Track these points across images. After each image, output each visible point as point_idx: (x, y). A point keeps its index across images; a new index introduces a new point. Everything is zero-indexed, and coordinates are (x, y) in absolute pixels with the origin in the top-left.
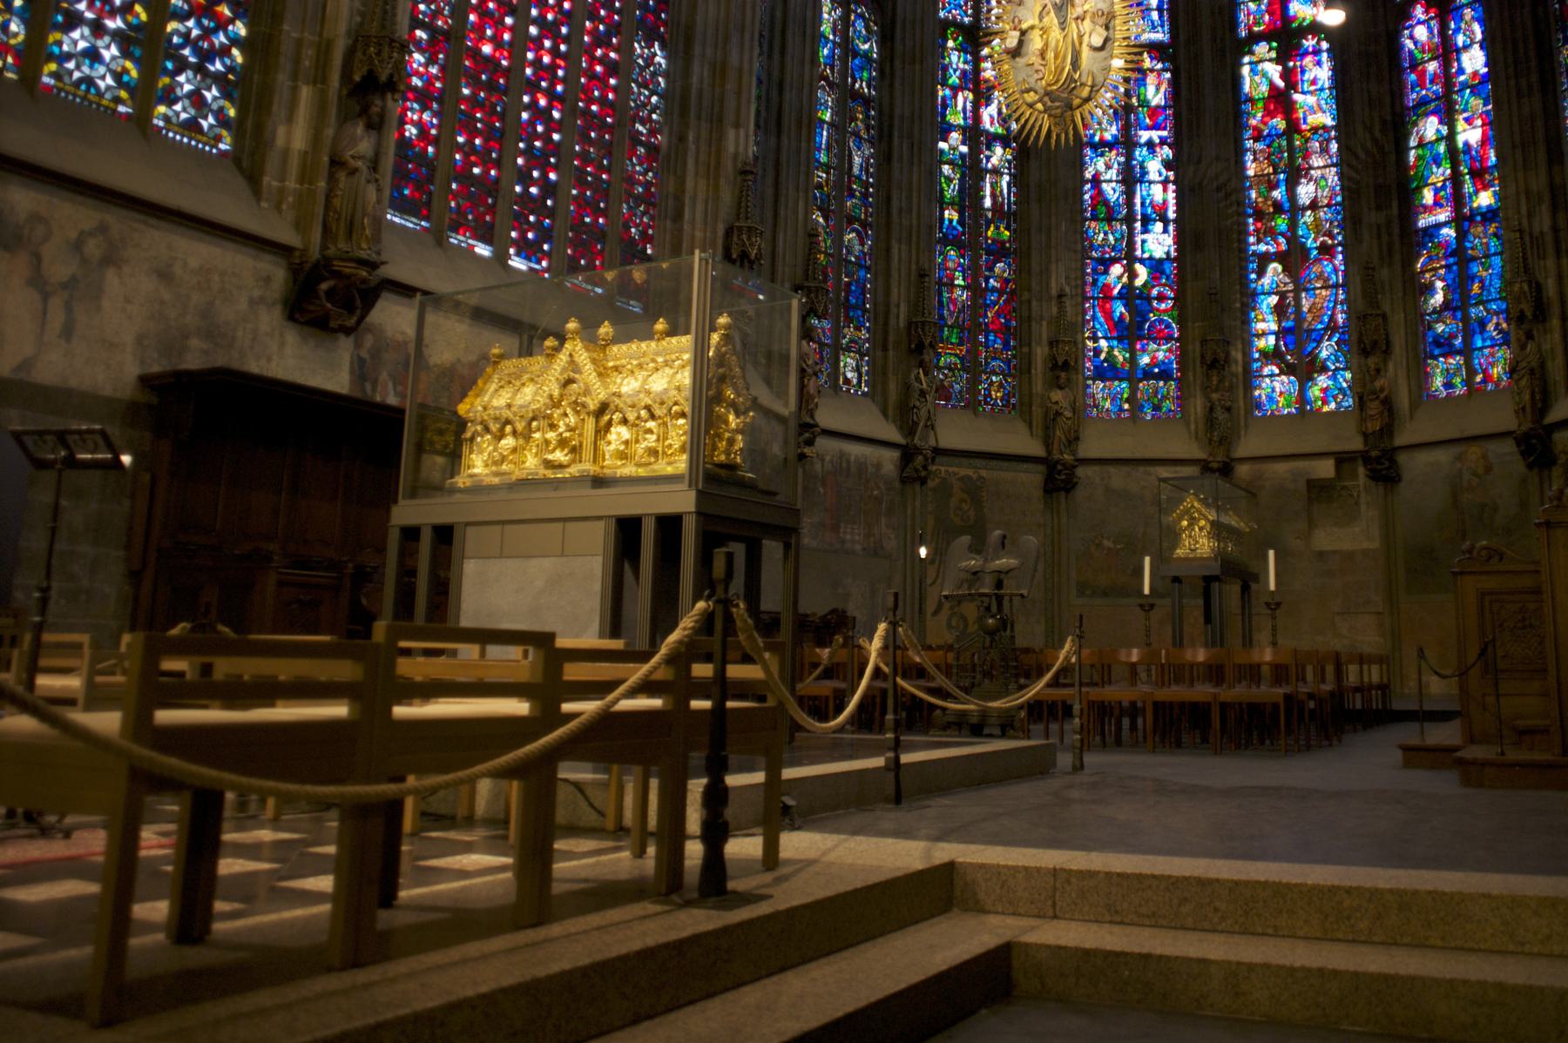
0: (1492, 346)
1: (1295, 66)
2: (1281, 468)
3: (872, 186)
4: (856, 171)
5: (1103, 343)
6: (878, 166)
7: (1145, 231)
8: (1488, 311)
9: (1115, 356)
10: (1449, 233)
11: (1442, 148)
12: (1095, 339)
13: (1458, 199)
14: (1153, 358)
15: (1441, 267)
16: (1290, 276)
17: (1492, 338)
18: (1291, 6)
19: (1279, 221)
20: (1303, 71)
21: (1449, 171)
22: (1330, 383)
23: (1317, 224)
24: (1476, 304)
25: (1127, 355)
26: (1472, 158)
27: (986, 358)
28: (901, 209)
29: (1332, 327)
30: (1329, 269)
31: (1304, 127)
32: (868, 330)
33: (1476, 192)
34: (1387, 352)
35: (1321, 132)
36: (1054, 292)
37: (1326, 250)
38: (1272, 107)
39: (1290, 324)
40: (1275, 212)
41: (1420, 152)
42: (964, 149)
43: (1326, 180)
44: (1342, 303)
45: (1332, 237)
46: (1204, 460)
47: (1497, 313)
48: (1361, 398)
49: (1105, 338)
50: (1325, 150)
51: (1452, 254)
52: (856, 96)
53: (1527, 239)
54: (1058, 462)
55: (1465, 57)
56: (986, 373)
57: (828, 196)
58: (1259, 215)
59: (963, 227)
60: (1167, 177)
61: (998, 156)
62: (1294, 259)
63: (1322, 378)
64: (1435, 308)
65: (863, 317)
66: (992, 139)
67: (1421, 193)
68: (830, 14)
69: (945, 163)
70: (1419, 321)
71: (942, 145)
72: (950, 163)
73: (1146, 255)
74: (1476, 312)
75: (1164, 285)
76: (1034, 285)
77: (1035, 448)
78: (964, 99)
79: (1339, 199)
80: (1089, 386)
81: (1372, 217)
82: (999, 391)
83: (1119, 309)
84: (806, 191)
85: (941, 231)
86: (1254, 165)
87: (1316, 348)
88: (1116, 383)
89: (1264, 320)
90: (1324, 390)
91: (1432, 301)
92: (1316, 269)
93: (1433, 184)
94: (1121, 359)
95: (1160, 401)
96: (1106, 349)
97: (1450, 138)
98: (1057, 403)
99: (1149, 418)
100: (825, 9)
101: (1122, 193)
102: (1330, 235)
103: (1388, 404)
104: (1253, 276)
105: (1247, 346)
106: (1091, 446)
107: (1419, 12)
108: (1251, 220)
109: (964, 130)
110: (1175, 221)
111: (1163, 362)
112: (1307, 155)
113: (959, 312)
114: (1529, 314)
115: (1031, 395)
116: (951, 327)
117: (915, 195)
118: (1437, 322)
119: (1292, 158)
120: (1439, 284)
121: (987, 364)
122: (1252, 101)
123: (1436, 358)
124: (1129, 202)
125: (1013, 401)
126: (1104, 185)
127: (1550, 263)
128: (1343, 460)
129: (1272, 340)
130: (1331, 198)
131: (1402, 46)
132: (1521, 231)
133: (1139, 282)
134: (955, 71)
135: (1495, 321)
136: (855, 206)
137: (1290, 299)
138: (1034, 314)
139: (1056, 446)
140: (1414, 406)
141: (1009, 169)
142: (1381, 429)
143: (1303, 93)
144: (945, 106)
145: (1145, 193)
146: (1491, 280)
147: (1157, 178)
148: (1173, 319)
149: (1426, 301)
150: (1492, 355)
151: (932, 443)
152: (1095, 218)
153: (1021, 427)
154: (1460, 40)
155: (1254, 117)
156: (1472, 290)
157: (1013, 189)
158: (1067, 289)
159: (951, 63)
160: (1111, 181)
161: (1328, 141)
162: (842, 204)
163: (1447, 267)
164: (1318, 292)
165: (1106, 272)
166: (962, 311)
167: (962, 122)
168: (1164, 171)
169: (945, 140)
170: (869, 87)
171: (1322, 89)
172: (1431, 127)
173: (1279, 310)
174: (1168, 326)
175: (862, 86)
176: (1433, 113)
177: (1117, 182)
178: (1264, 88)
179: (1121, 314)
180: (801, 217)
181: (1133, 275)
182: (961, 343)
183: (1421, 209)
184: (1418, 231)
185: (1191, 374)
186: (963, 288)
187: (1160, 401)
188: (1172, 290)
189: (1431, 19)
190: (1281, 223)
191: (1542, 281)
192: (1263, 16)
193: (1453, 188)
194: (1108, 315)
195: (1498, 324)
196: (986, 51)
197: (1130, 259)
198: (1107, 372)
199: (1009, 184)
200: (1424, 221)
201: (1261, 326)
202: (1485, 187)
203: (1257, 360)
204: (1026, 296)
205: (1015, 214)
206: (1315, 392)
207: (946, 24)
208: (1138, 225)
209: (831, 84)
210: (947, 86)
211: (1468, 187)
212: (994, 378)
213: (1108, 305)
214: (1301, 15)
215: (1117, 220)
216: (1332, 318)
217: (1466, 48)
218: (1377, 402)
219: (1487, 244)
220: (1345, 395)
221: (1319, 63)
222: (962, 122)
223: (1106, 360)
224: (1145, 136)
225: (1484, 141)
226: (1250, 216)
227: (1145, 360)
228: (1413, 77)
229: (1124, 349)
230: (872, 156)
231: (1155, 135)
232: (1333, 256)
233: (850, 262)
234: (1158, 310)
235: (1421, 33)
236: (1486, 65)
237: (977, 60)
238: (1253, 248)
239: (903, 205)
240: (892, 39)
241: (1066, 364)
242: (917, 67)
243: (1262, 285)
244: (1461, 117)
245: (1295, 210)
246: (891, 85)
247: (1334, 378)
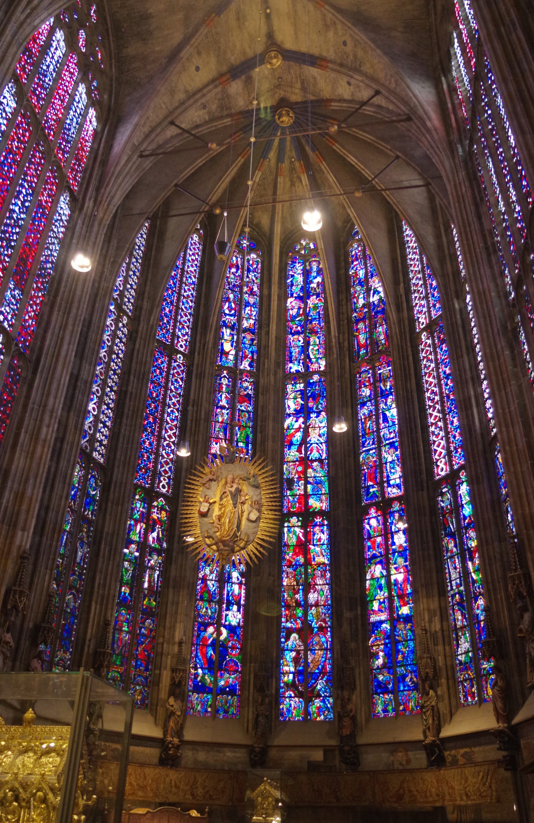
0: (408, 690)
1: (310, 531)
2: (294, 754)
3: (85, 569)
4: (78, 560)
5: (200, 671)
6: (91, 558)
7: (228, 609)
8: (406, 670)
9: (206, 679)
10: (386, 626)
11: (383, 581)
12: (196, 668)
13: (391, 609)
14: (227, 682)
15: (382, 644)
16: (303, 642)
17: (409, 686)
18: (310, 501)
19: (298, 611)
20: (314, 535)
21: (386, 594)
22: (321, 704)
23: (318, 615)
24: (400, 666)
25: (212, 679)
26: (398, 588)
27: (134, 675)
28: (99, 584)
29: (322, 672)
30: (323, 639)
31: (313, 563)
32: (71, 653)
33: (401, 606)
34: (354, 689)
35: (321, 566)
36: (177, 640)
37: (321, 628)
38: (297, 551)
39: (301, 668)
40: (296, 606)
41: (372, 582)
42: (137, 554)
43: (323, 592)
44: (329, 660)
45: (326, 623)
46: (252, 746)
47: (411, 672)
48: (339, 715)
49: (202, 668)
50: (323, 576)
51: (388, 637)
52: (85, 519)
53: (428, 634)
54: (170, 742)
55: (396, 537)
56: (133, 684)
57: (62, 572)
58: (288, 607)
59: (131, 598)
60: (241, 581)
61: (154, 560)
63: (317, 701)
64: (378, 666)
65: (69, 644)
66: (153, 550)
67: (372, 603)
68: (78, 473)
69: (126, 561)
71: (126, 551)
72: (129, 561)
73: (227, 623)
74: (401, 670)
75: (236, 640)
76: (166, 634)
77: (156, 733)
79: (329, 602)
80: (190, 696)
81: (347, 614)
82: (139, 695)
83: (210, 652)
84: (52, 570)
85: (119, 596)
86: (286, 580)
87: (314, 683)
88: (205, 695)
89: (287, 665)
90: (319, 708)
91: (377, 662)
92: (316, 639)
93: (379, 600)
94: (209, 681)
95: (229, 708)
96: (201, 675)
97: (388, 576)
98: (172, 706)
99: (221, 717)
100: (77, 470)
101: (218, 587)
102: (324, 621)
103: (354, 719)
104: (283, 640)
105: (279, 680)
106: (189, 735)
107: (373, 511)
108: (283, 609)
109: (138, 543)
110: (244, 605)
111: (232, 685)
112: (314, 577)
113: (123, 647)
114: (431, 675)
115: (158, 699)
116: (118, 655)
117: (108, 577)
118: (379, 674)
119: (306, 578)
120: (381, 654)
121: (135, 678)
122: (288, 546)
123: (379, 695)
124: (221, 594)
125: (146, 702)
126: (208, 582)
127: (440, 648)
128: (327, 751)
129: (291, 676)
130: (325, 602)
131: (364, 528)
132: (426, 630)
133: (222, 638)
134: (138, 512)
135: (410, 676)
136: (74, 580)
137: (302, 655)
138: (164, 652)
139: (169, 732)
140: (367, 721)
141: (159, 567)
142: (350, 734)
143: (314, 545)
144: (130, 530)
145: (229, 589)
146: (408, 654)
147: (236, 581)
148: (239, 660)
149: (374, 662)
150: (409, 695)
151: (100, 726)
152: (202, 599)
153: (151, 719)
155: (288, 554)
156: (397, 658)
157: (160, 579)
158: (184, 638)
159: (136, 507)
160: (212, 580)
161: (325, 571)
162: (68, 578)
163: (385, 644)
164: (316, 652)
165: (205, 630)
166: (124, 646)
167: (138, 539)
168: (240, 577)
169: (128, 548)
170: (92, 514)
171: (323, 544)
173: (296, 660)
174: (236, 664)
175: (88, 513)
176: (380, 562)
177: (215, 581)
178: (294, 540)
179: (211, 654)
180: (46, 584)
181: (220, 634)
182: (122, 665)
183: (372, 612)
184: (370, 623)
185: (247, 693)
186: (127, 632)
187: (229, 708)
188: (239, 643)
189: (379, 516)
190: (299, 612)
191: (436, 657)
192: (296, 504)
193: (389, 602)
194: (205, 655)
195: (411, 679)
196: (155, 504)
197: (218, 624)
198: (201, 688)
199: (158, 576)
200: (374, 618)
201: (286, 668)
202: (405, 605)
203: (282, 688)
204: (161, 640)
205: (160, 592)
206: (313, 709)
207: (136, 486)
208: (224, 606)
209: (72, 511)
210: (133, 519)
211: (397, 603)
212: (137, 687)
213: (204, 650)
214: (314, 506)
215: (213, 602)
217: (396, 532)
218: (348, 718)
219: (406, 635)
220: (329, 711)
221: (322, 532)
222: (138, 539)
223: (200, 681)
225: (406, 580)
226: (283, 607)
227: (222, 683)
228: (369, 544)
229: (211, 675)
230: (88, 552)
233: (67, 612)
234: (231, 654)
236: (406, 542)
237: (150, 507)
238: (284, 624)
239: (102, 582)
240: (109, 490)
241: (180, 682)
242: (120, 507)
243: (288, 645)
244: (393, 567)
245: (306, 606)
246: (105, 516)
247: (323, 701)
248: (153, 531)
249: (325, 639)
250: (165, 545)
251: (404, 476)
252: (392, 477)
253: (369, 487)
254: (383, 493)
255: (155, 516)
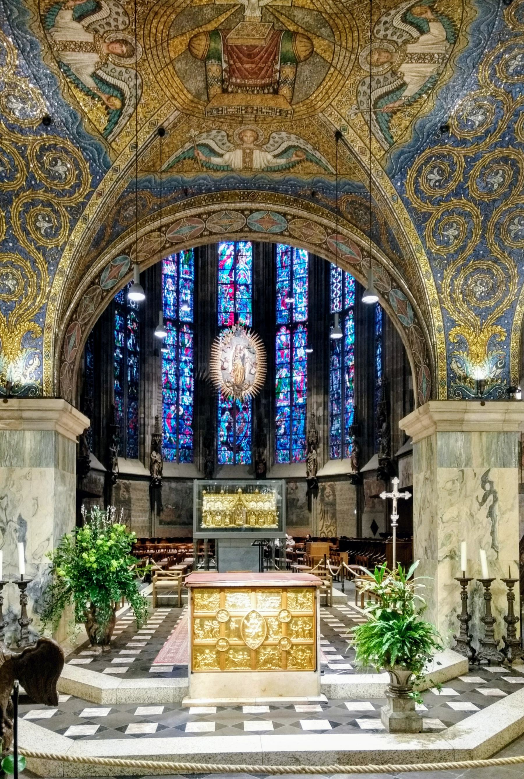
29: (245, 436)
37: (245, 409)
39: (231, 433)
42: (121, 356)
55: (298, 351)
62: (234, 410)
66: (130, 353)
70: (276, 438)
72: (117, 361)
78: (121, 336)
97: (291, 377)
154: (297, 345)
172: (284, 372)
173: (228, 429)
216: (246, 433)
224: (184, 358)
231: (187, 358)
232: (247, 412)
235: (283, 338)
248: (129, 338)
249: (247, 415)
250: (138, 349)
251: (310, 307)
252: (299, 305)
253: (281, 311)
254: (291, 317)
255: (130, 326)
